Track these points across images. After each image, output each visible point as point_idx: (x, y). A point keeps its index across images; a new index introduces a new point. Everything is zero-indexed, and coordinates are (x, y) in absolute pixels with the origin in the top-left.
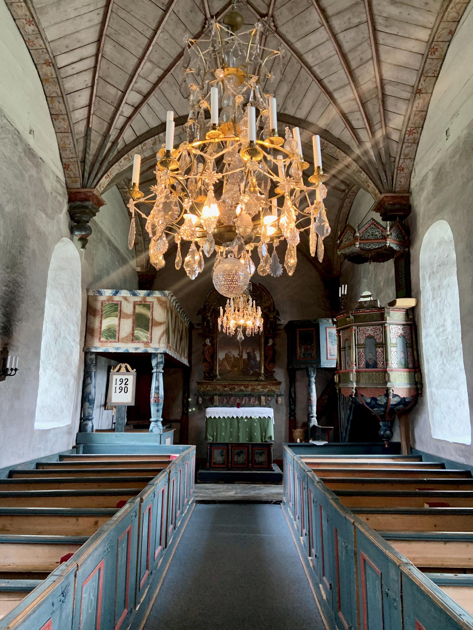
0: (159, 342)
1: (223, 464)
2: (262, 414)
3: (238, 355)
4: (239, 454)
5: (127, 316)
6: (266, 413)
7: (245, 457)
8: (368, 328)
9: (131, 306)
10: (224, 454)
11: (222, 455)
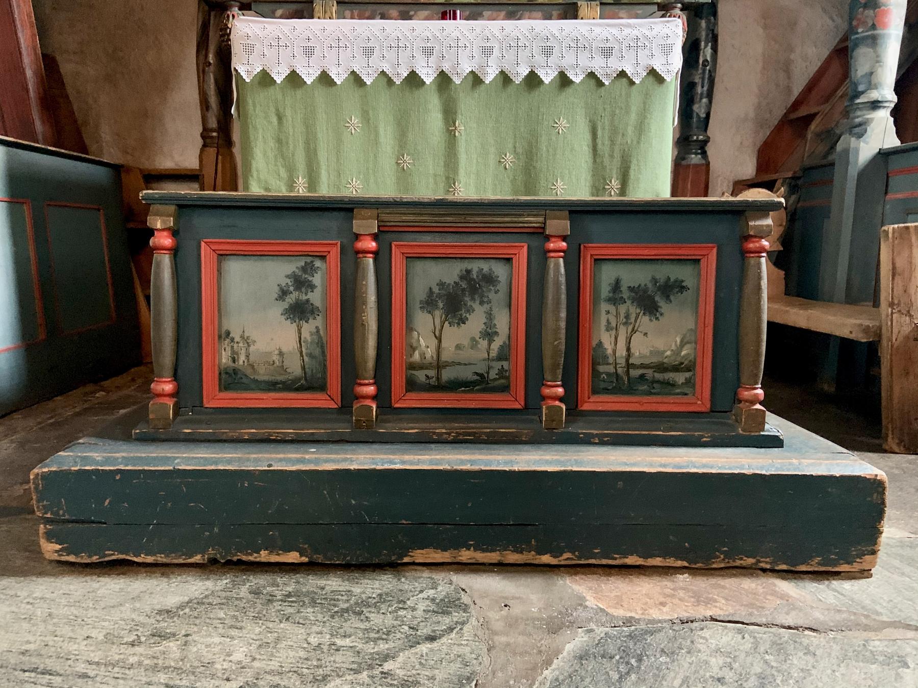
1: (311, 383)
2: (607, 52)
4: (452, 304)
6: (636, 45)
7: (502, 323)
10: (315, 297)
11: (299, 312)
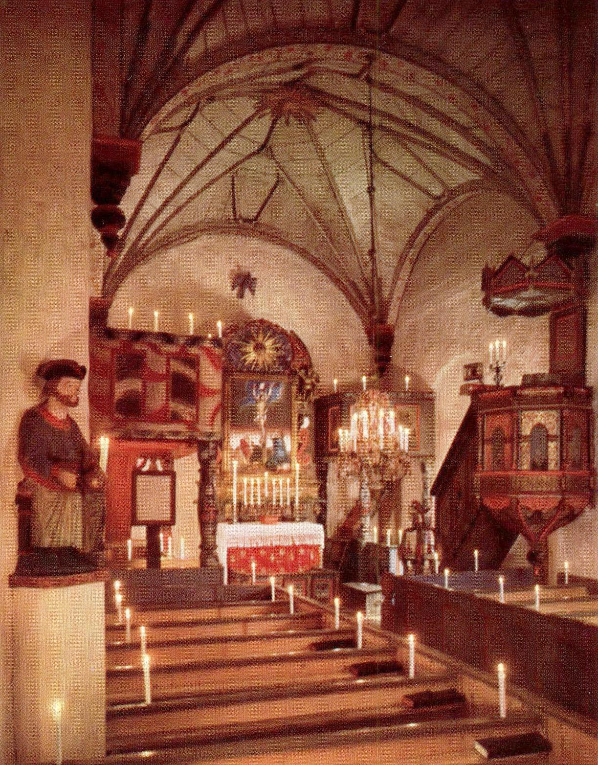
0: (212, 424)
3: (260, 441)
5: (157, 377)
8: (536, 413)
9: (163, 359)
